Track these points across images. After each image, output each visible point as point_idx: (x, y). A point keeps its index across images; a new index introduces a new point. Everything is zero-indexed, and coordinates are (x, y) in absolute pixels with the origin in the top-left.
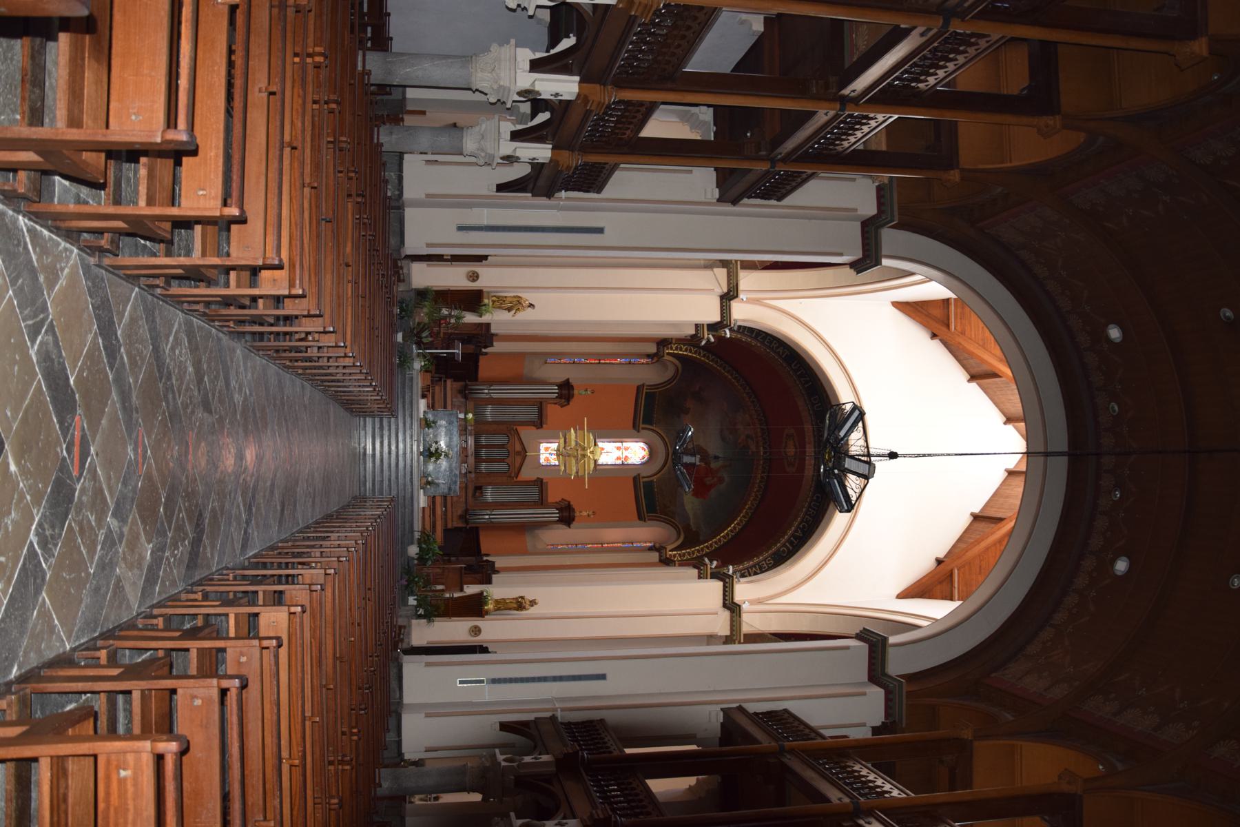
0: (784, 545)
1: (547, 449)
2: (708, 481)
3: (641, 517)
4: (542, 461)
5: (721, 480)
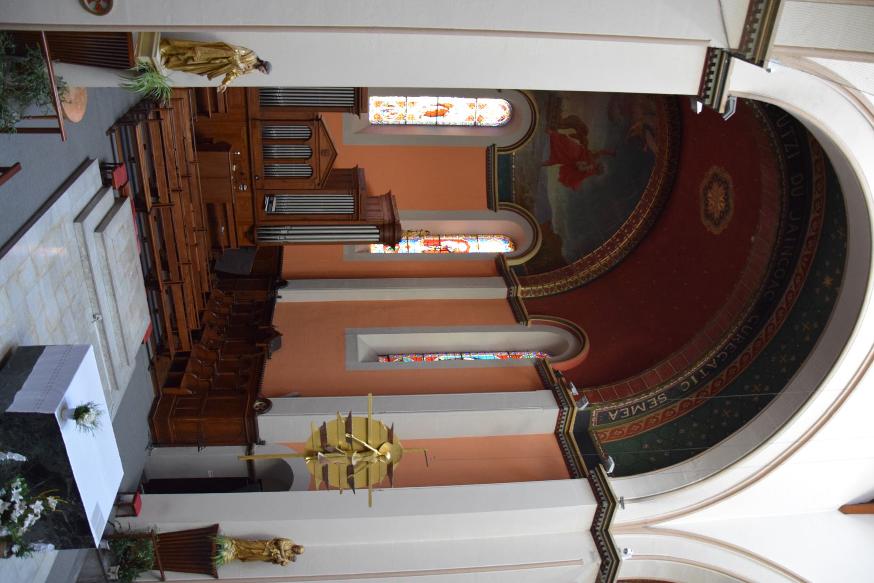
0: (688, 379)
1: (378, 104)
2: (582, 165)
3: (490, 206)
4: (372, 118)
5: (598, 170)
